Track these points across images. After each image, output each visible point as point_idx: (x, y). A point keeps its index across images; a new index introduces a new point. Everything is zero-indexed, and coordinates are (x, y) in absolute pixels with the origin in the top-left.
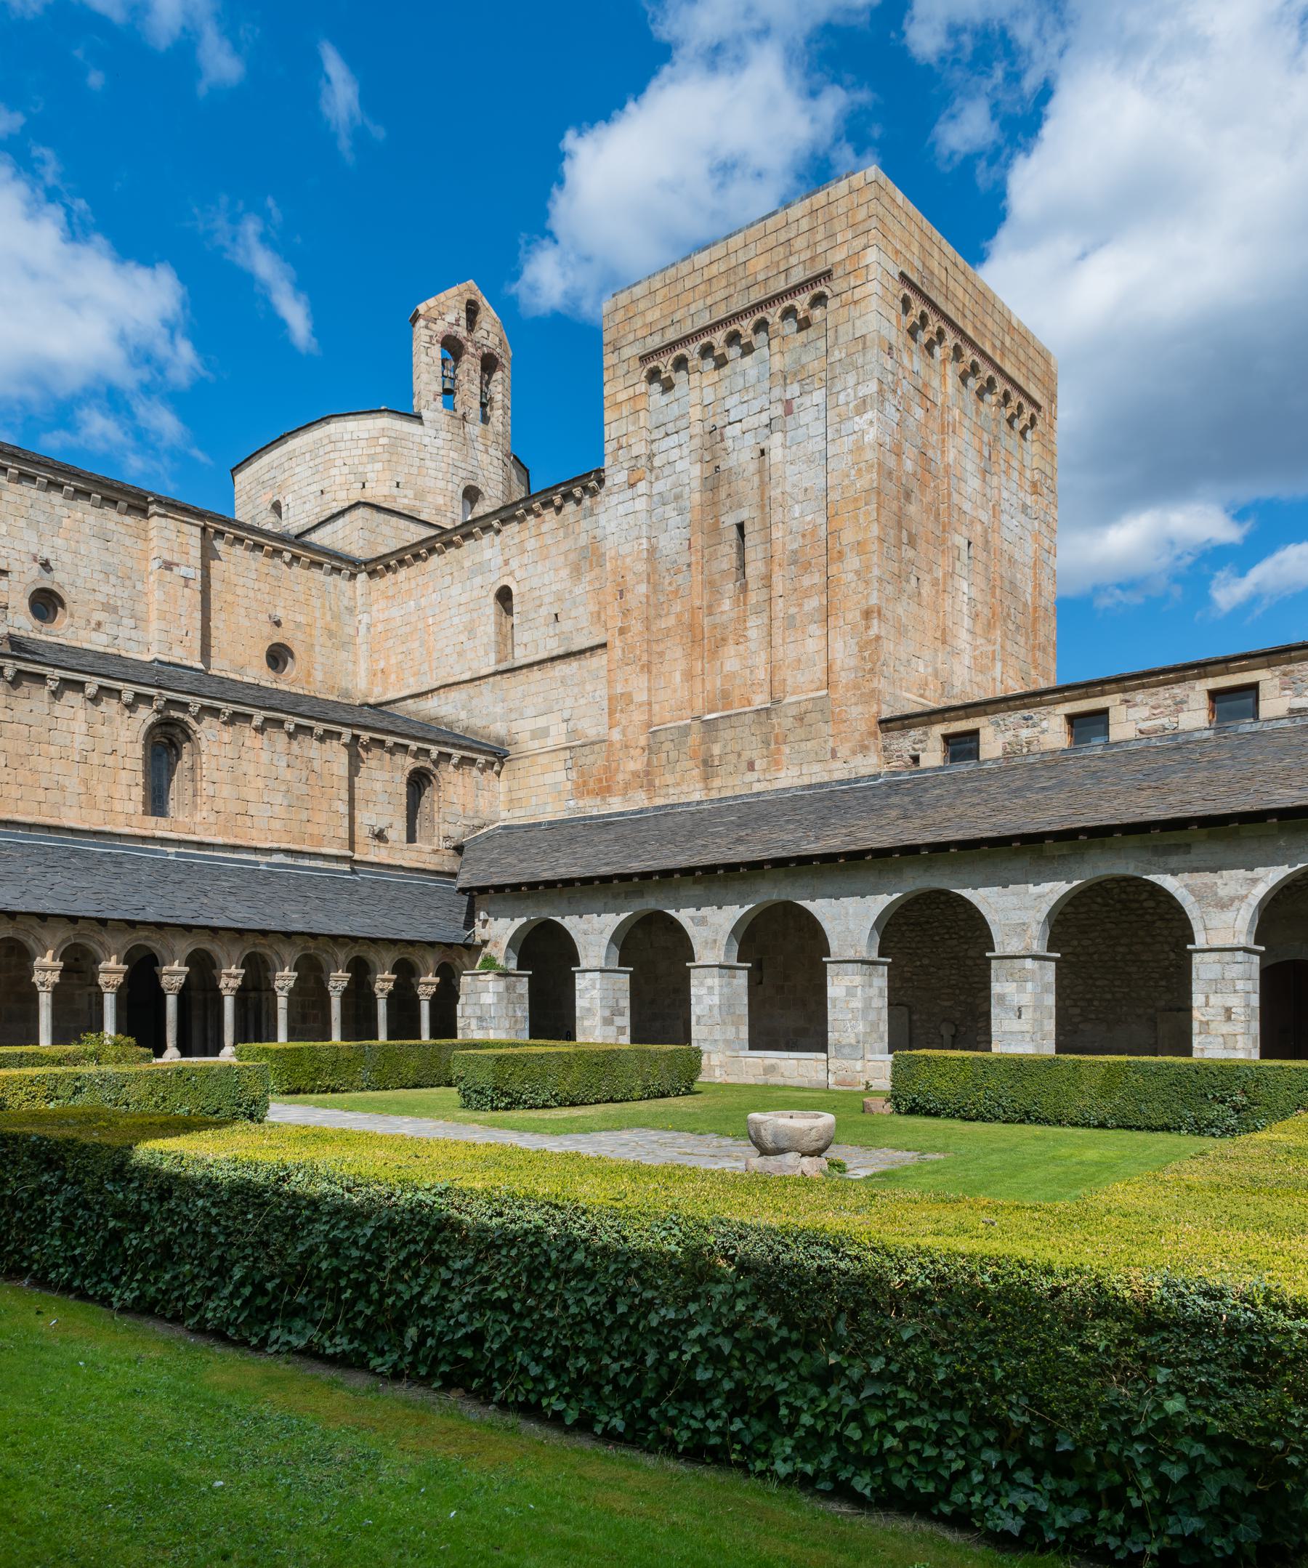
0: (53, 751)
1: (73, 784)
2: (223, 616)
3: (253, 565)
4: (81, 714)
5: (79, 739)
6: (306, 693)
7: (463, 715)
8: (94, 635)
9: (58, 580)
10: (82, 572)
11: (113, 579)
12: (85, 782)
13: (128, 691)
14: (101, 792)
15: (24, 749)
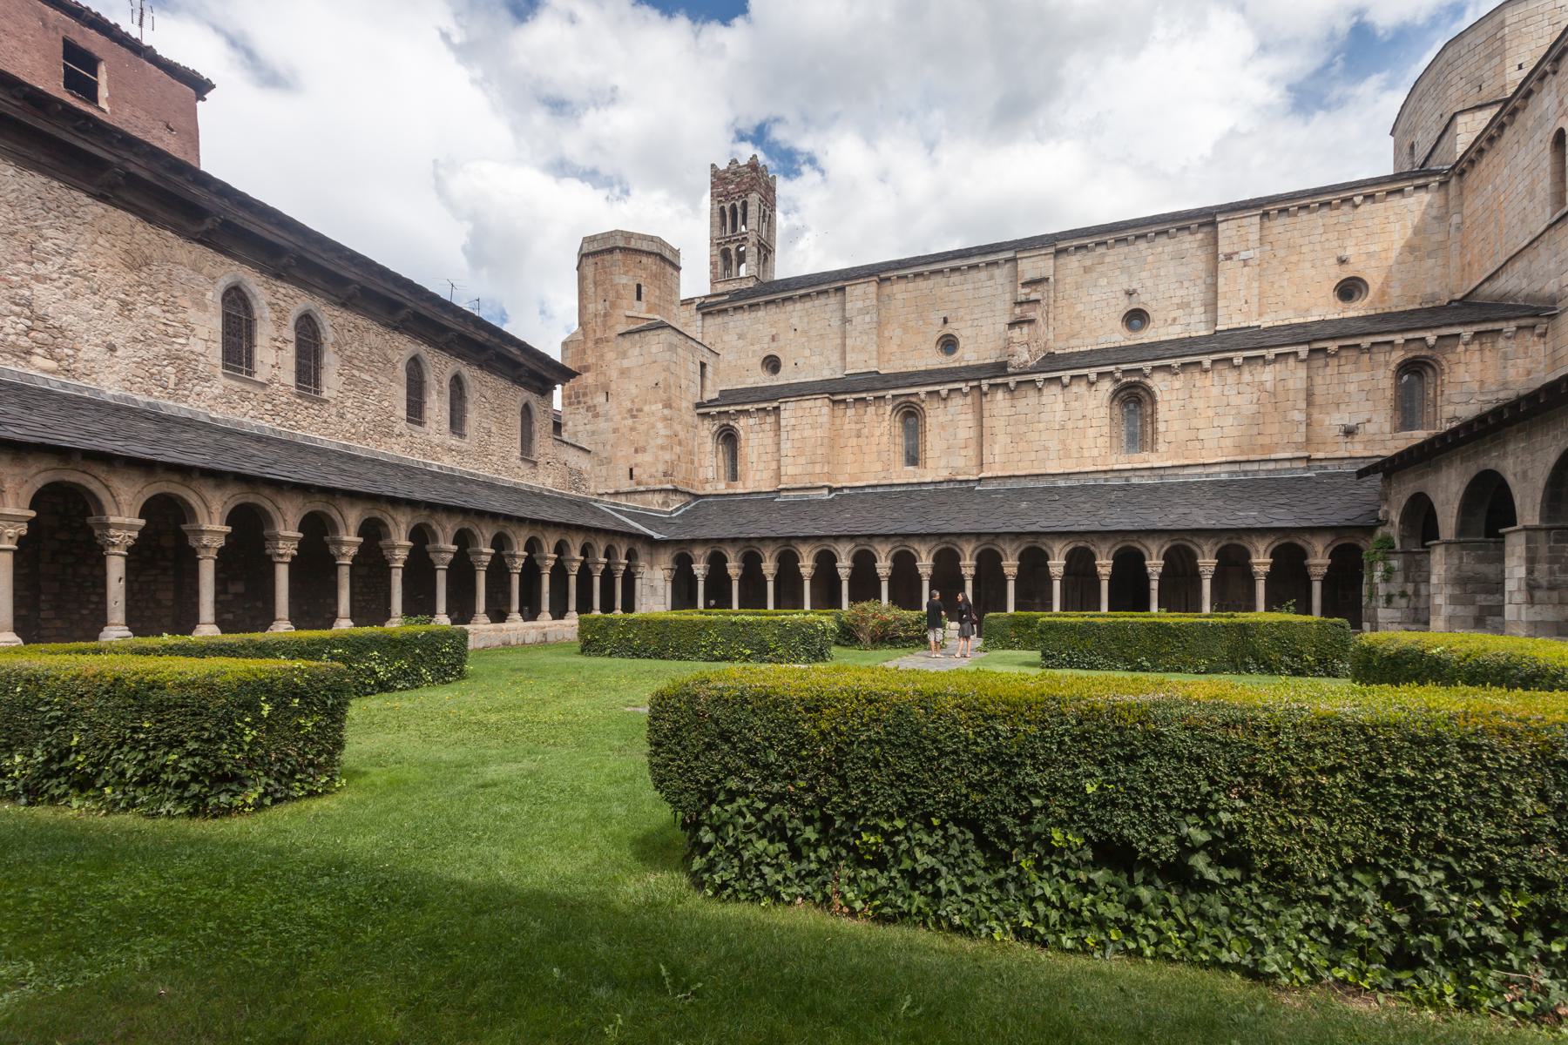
0: (1041, 426)
1: (1054, 445)
2: (1287, 275)
3: (1320, 222)
4: (1060, 398)
5: (1058, 415)
6: (1379, 311)
7: (1524, 285)
8: (1171, 329)
9: (1144, 301)
10: (1161, 288)
11: (1186, 284)
12: (1063, 442)
13: (1092, 373)
14: (1074, 447)
15: (1025, 429)
